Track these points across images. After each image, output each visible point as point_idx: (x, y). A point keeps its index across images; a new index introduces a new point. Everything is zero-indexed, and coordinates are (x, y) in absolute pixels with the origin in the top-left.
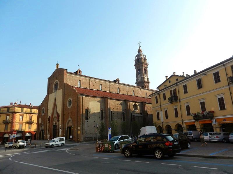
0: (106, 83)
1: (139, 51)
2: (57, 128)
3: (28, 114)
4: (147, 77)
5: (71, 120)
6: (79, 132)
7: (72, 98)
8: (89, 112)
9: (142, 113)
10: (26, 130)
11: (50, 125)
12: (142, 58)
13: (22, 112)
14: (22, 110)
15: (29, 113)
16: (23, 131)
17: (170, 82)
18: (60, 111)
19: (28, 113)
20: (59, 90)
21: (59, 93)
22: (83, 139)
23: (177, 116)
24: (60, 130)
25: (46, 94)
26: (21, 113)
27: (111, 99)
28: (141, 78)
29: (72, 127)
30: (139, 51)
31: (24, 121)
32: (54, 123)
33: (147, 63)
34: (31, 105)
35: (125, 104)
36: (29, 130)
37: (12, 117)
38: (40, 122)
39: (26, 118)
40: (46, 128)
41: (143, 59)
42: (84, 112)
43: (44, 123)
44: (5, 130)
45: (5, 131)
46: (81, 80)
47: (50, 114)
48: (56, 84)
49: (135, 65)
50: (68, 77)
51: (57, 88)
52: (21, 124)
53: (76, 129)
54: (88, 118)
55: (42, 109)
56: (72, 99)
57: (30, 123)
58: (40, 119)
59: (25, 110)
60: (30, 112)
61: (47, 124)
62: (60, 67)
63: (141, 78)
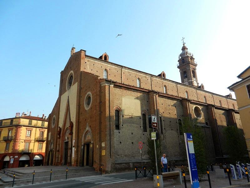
0: (146, 77)
1: (184, 48)
2: (70, 146)
3: (38, 129)
4: (197, 81)
5: (90, 130)
6: (104, 153)
8: (121, 116)
9: (208, 123)
10: (35, 151)
11: (61, 142)
12: (188, 57)
13: (30, 126)
14: (30, 123)
15: (40, 128)
16: (30, 152)
18: (74, 119)
19: (38, 127)
21: (75, 88)
22: (112, 166)
24: (73, 148)
26: (28, 126)
29: (91, 142)
30: (184, 48)
31: (33, 138)
32: (66, 138)
33: (195, 63)
34: (44, 118)
35: (181, 106)
36: (40, 151)
37: (15, 131)
38: (49, 139)
39: (36, 134)
40: (55, 147)
41: (189, 58)
42: (113, 113)
43: (54, 140)
45: (6, 152)
46: (108, 70)
47: (61, 125)
48: (71, 77)
49: (178, 67)
50: (88, 63)
51: (72, 84)
52: (28, 142)
53: (97, 146)
54: (121, 126)
55: (53, 118)
56: (91, 94)
57: (40, 141)
58: (50, 134)
59: (34, 122)
60: (42, 125)
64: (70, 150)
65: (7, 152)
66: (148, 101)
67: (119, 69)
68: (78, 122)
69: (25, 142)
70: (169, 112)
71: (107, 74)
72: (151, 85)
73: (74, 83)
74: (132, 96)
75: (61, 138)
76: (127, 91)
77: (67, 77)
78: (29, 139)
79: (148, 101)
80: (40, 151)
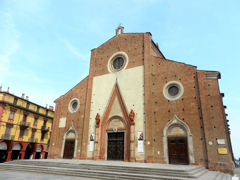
10: (16, 139)
16: (10, 139)
20: (126, 69)
69: (6, 126)
75: (100, 127)
78: (11, 122)
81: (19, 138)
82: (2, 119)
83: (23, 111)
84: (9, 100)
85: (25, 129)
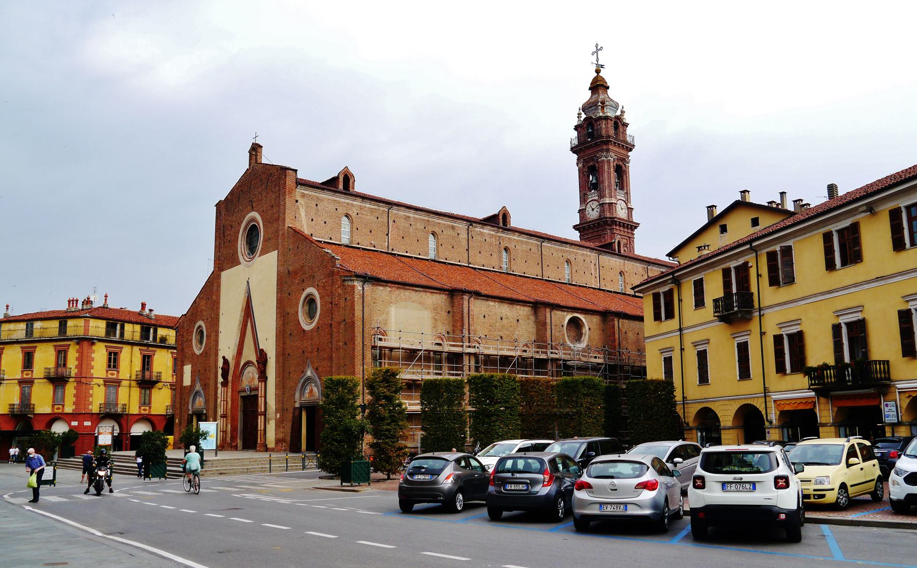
0: (453, 228)
1: (598, 86)
4: (627, 201)
7: (318, 290)
10: (134, 409)
16: (119, 410)
17: (724, 229)
18: (269, 345)
20: (260, 255)
23: (745, 373)
25: (210, 268)
27: (478, 295)
28: (602, 205)
30: (598, 86)
38: (187, 381)
40: (212, 406)
43: (205, 386)
44: (53, 406)
45: (56, 411)
46: (354, 215)
48: (253, 232)
49: (574, 150)
58: (187, 369)
61: (216, 389)
62: (268, 157)
63: (602, 205)
64: (263, 417)
65: (58, 409)
66: (449, 312)
67: (383, 208)
68: (282, 355)
69: (105, 385)
70: (501, 334)
71: (352, 228)
72: (468, 250)
73: (264, 252)
74: (413, 302)
75: (230, 384)
76: (401, 291)
77: (240, 224)
79: (449, 312)
80: (145, 410)
81: (140, 407)
82: (92, 372)
83: (139, 347)
84: (97, 331)
85: (152, 388)
